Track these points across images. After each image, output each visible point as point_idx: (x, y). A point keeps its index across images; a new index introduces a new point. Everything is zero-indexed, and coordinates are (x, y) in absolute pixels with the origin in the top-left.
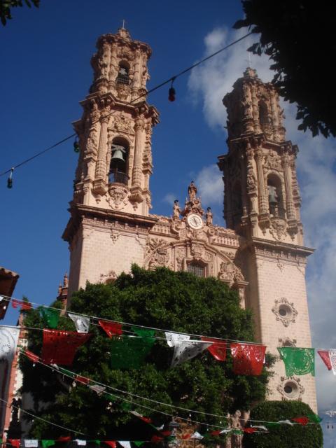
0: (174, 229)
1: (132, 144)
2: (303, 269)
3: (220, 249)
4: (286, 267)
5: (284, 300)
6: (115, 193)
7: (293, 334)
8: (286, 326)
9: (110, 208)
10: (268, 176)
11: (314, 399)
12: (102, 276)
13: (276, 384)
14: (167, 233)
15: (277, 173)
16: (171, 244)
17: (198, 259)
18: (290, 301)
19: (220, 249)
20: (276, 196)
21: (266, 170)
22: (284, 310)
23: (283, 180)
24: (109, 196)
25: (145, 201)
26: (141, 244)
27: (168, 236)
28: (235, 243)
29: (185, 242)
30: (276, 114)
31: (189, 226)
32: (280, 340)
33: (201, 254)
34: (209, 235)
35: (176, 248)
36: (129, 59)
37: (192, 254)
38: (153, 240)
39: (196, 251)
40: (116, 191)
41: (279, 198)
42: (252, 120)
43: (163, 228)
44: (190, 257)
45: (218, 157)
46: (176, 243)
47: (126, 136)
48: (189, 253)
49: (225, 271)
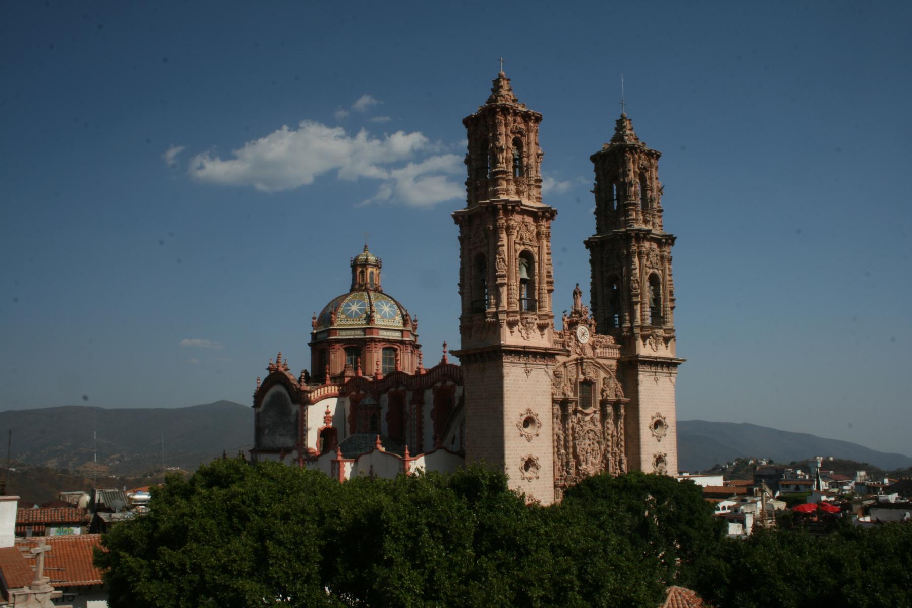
1: (536, 258)
5: (659, 415)
6: (528, 323)
16: (565, 363)
18: (663, 415)
24: (521, 326)
28: (616, 353)
29: (576, 360)
31: (578, 341)
34: (594, 348)
36: (523, 135)
37: (583, 374)
42: (635, 204)
44: (581, 377)
47: (530, 248)
48: (580, 372)
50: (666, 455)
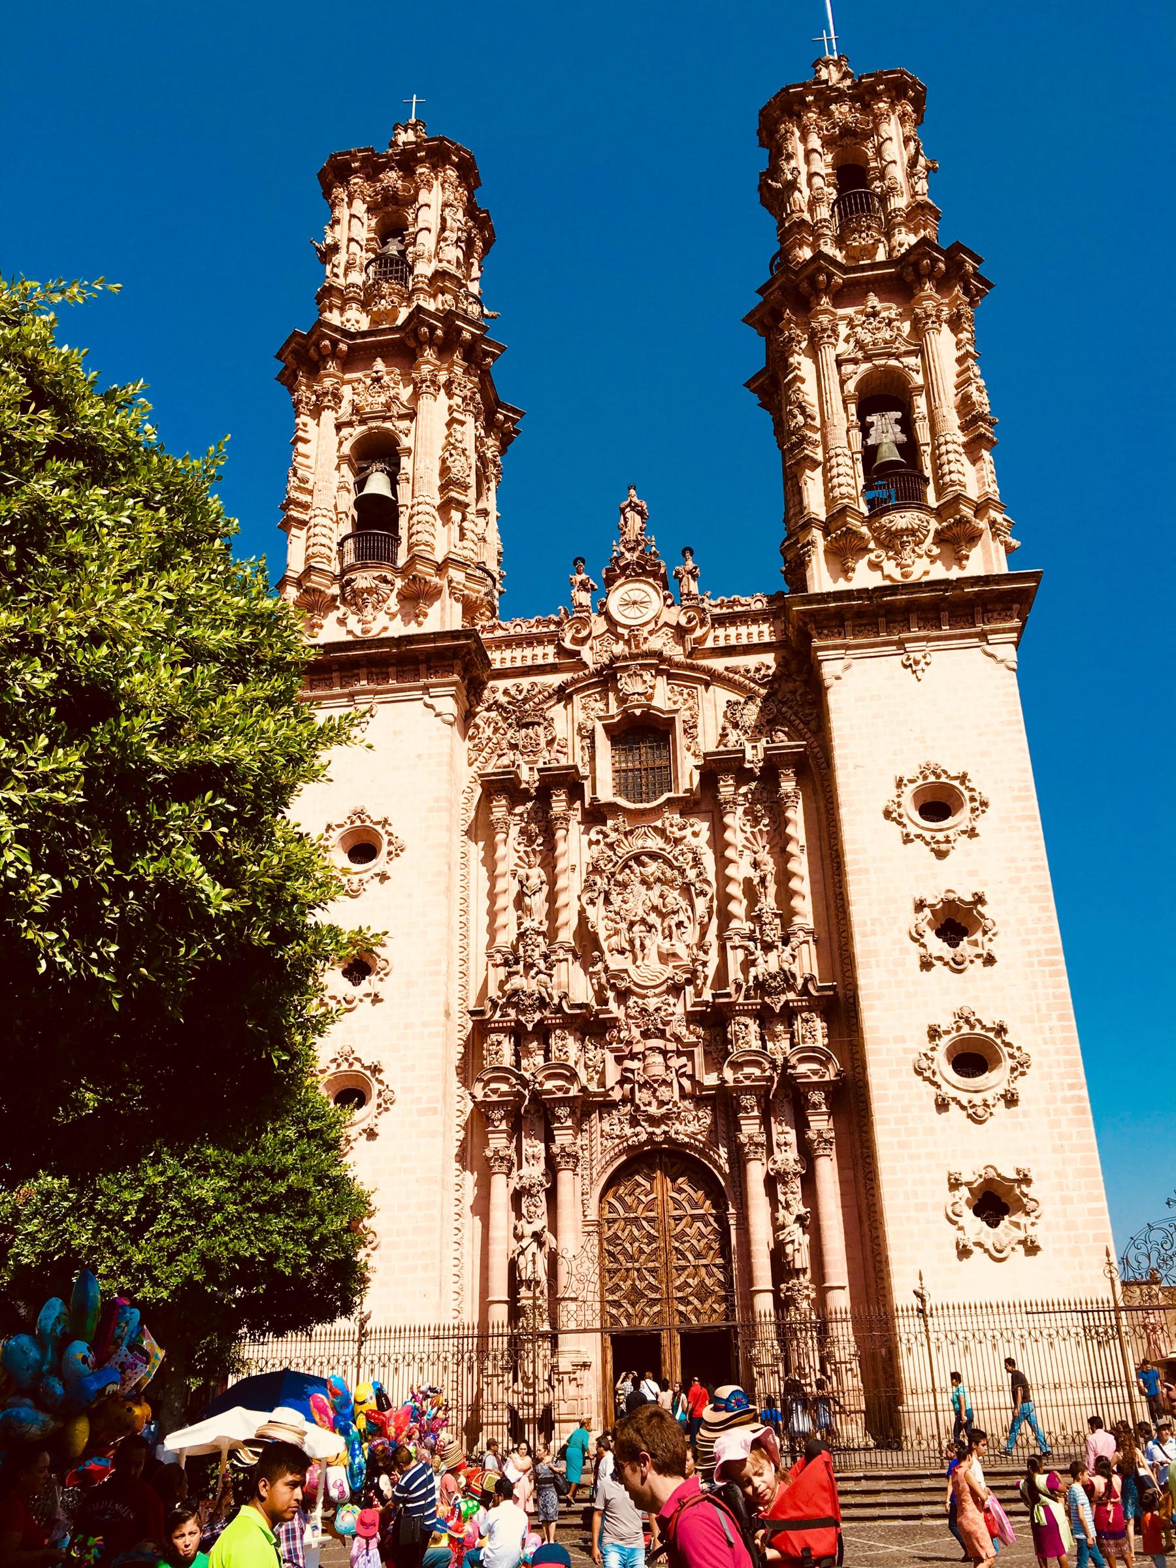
0: (567, 644)
2: (1009, 653)
3: (718, 664)
4: (935, 657)
7: (973, 873)
8: (941, 855)
9: (350, 638)
10: (860, 386)
11: (1072, 1087)
12: (329, 827)
13: (906, 1051)
14: (551, 660)
15: (893, 362)
16: (561, 689)
17: (638, 712)
19: (718, 664)
20: (902, 438)
21: (848, 368)
22: (938, 803)
23: (919, 379)
25: (446, 591)
26: (438, 715)
27: (553, 669)
29: (598, 673)
30: (898, 173)
32: (920, 906)
33: (650, 698)
34: (680, 632)
35: (576, 698)
38: (506, 692)
39: (630, 689)
40: (356, 585)
41: (910, 448)
43: (539, 650)
45: (747, 385)
46: (574, 681)
49: (736, 726)
50: (980, 900)
